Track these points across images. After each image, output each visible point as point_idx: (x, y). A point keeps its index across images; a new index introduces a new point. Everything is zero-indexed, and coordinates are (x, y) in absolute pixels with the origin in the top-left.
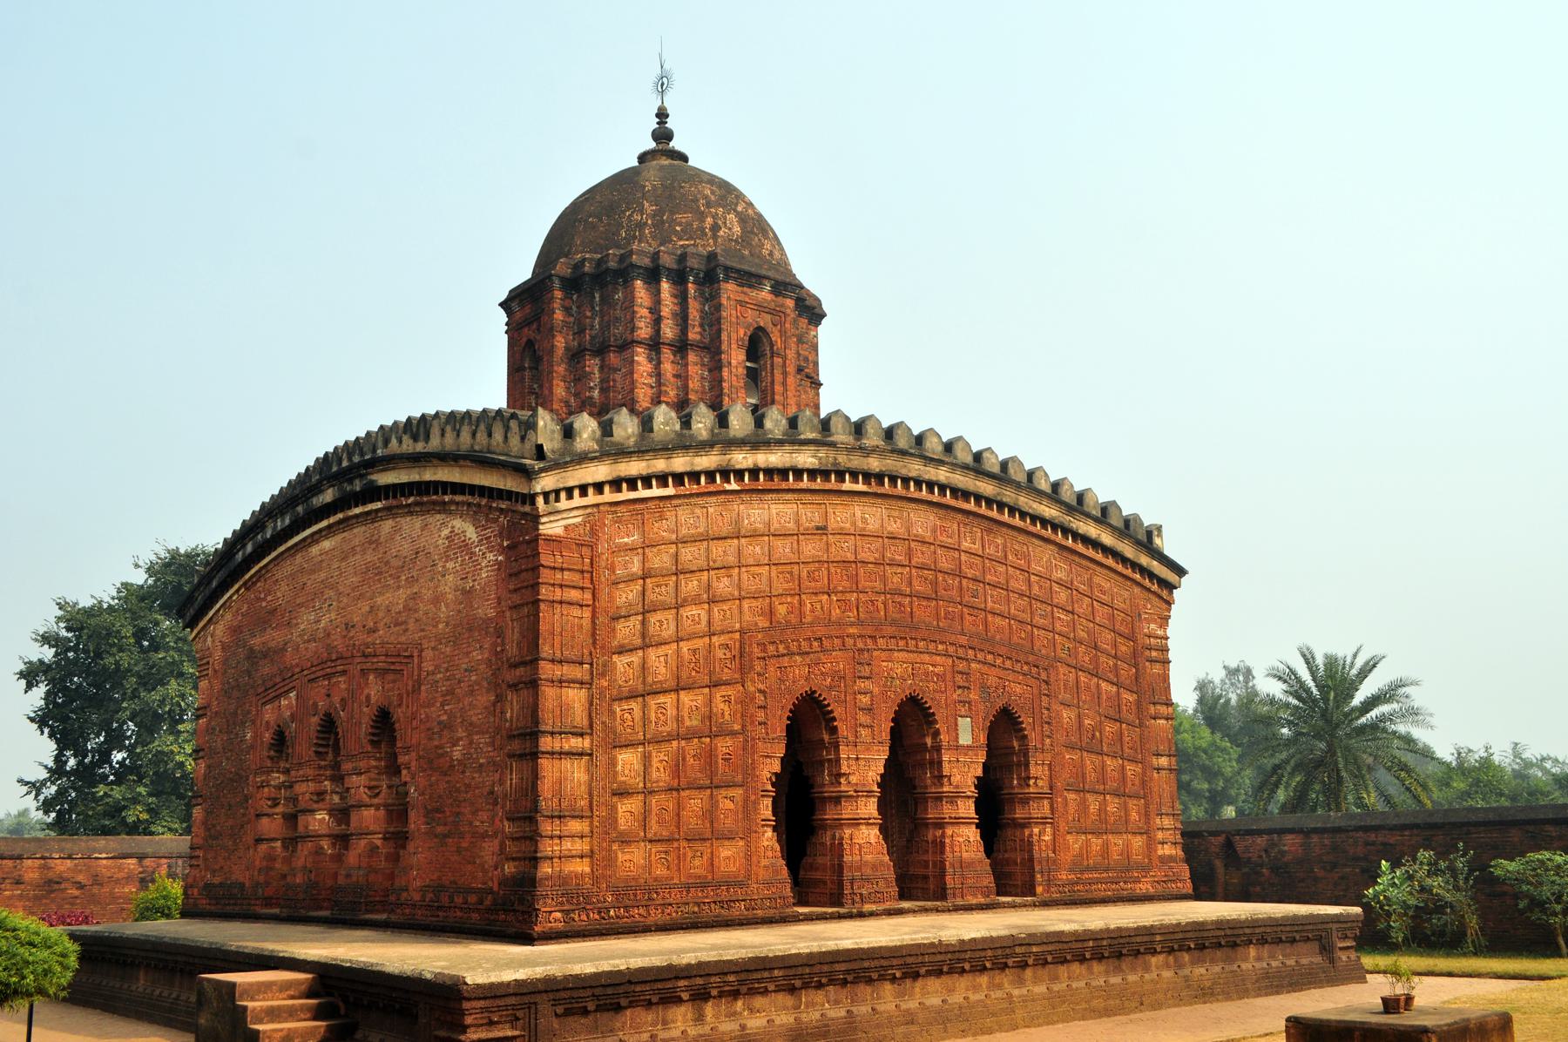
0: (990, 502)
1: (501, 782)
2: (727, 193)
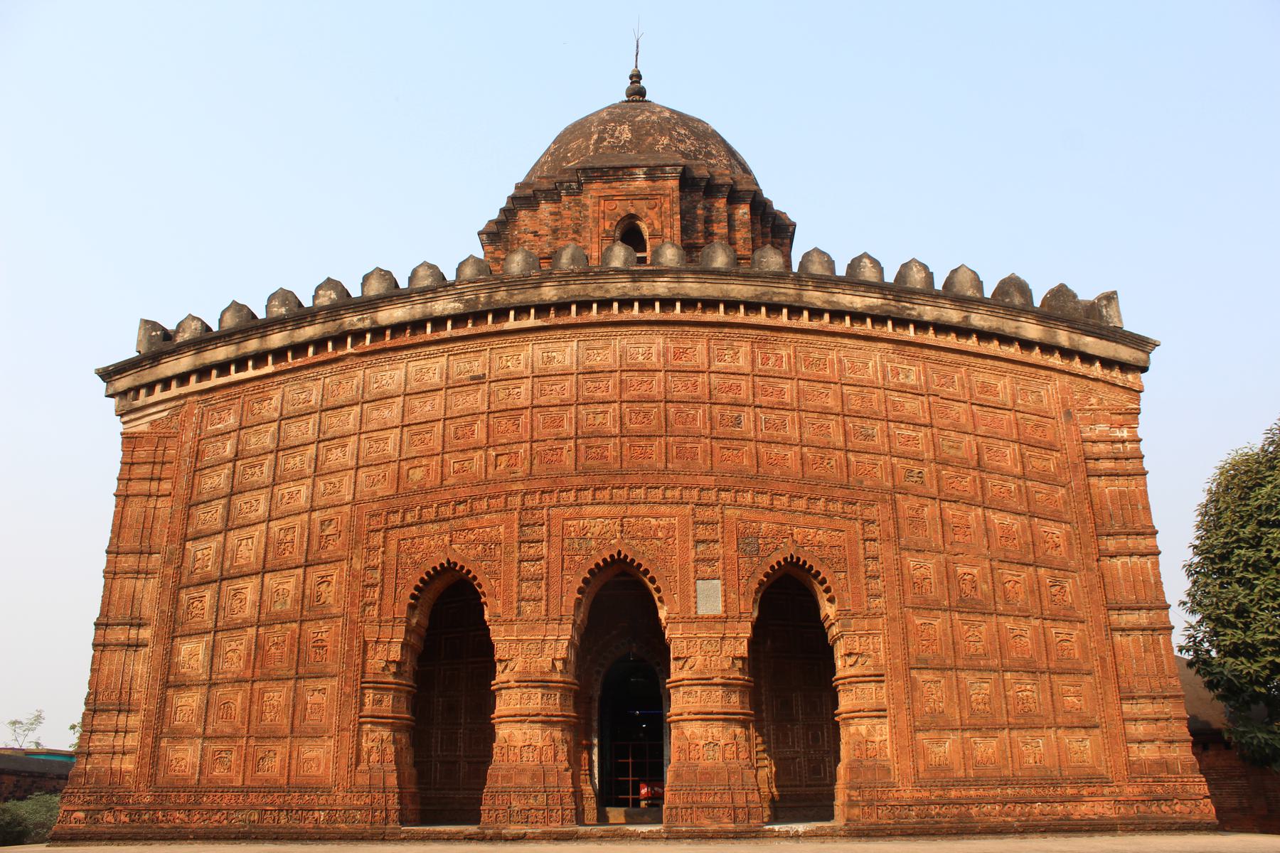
0: (752, 307)
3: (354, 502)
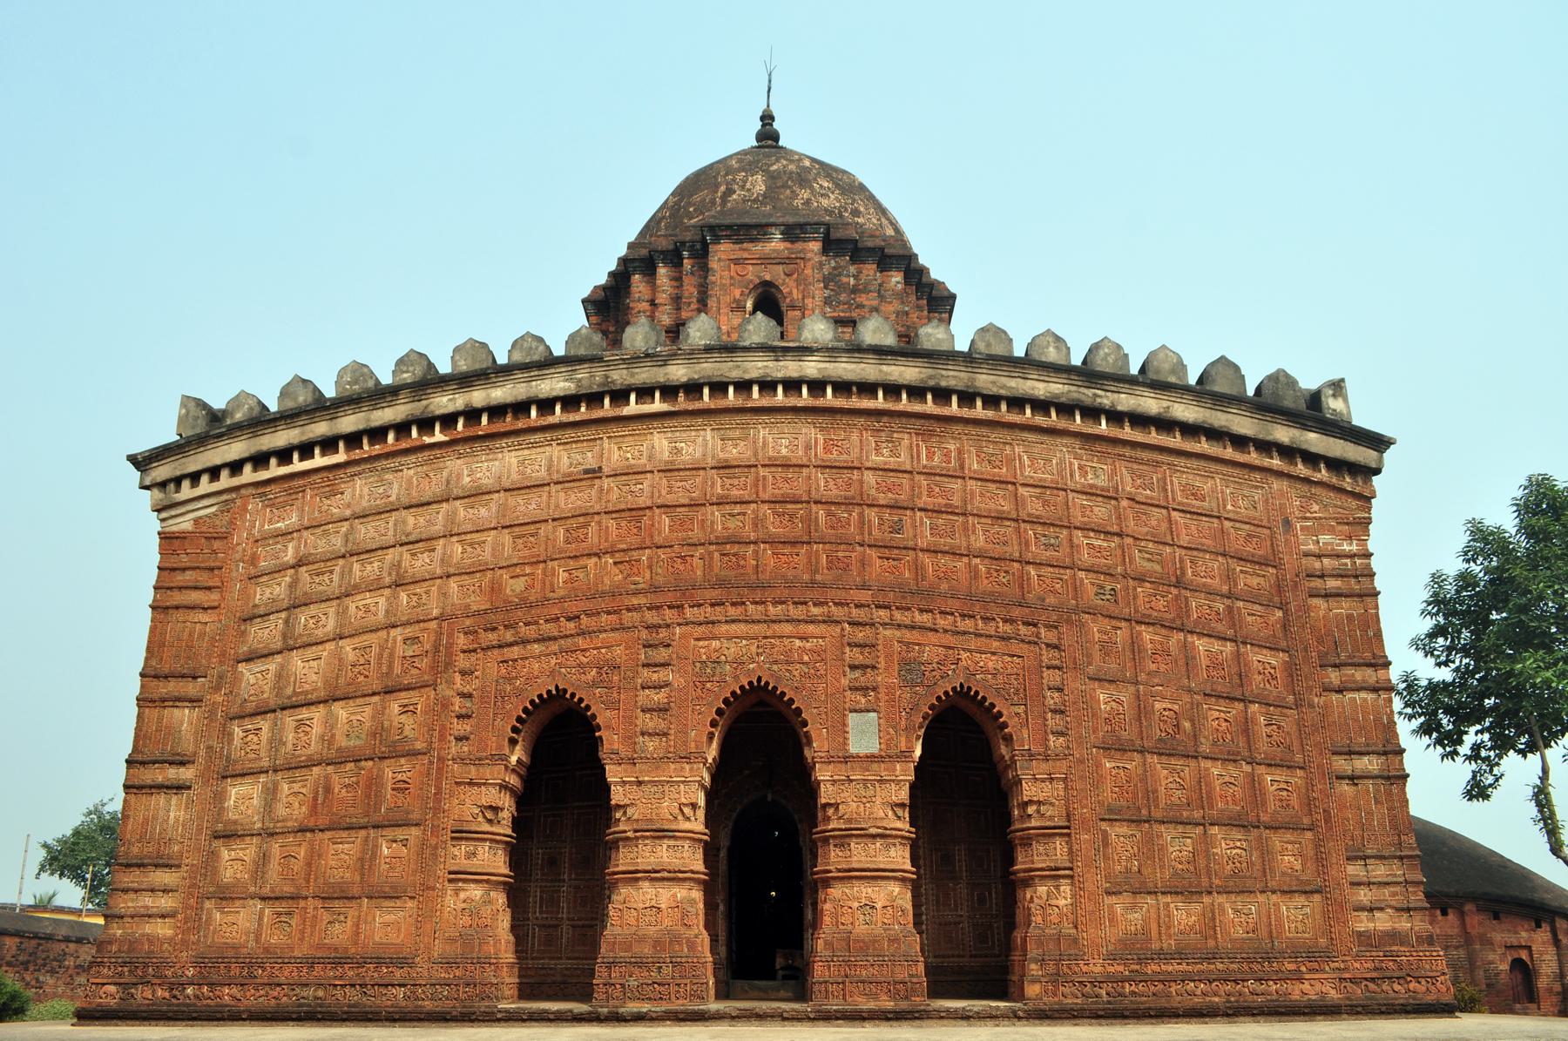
0: (917, 392)
3: (440, 618)
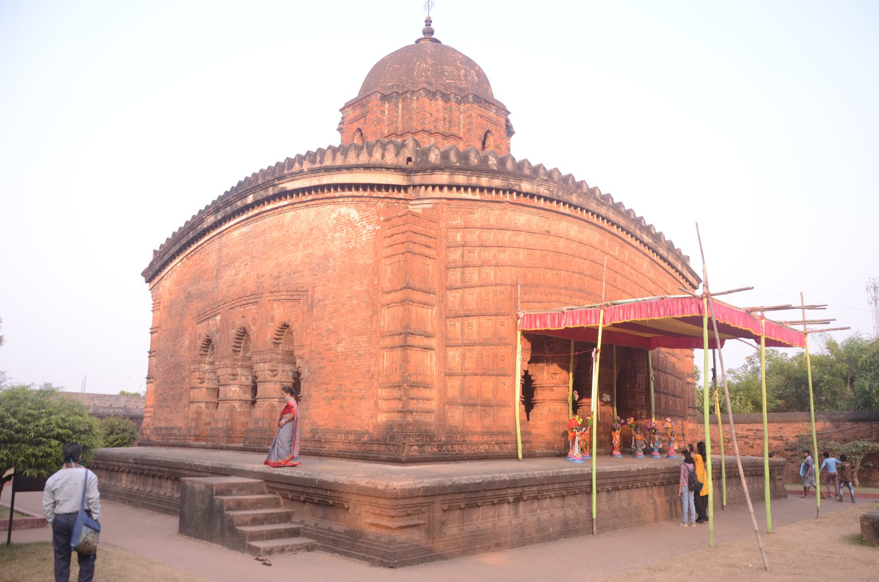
1: (376, 364)
2: (469, 63)
